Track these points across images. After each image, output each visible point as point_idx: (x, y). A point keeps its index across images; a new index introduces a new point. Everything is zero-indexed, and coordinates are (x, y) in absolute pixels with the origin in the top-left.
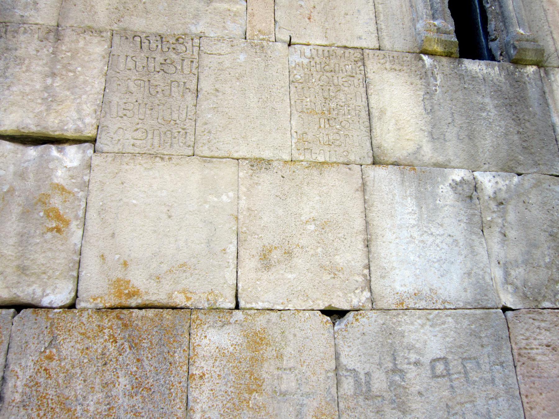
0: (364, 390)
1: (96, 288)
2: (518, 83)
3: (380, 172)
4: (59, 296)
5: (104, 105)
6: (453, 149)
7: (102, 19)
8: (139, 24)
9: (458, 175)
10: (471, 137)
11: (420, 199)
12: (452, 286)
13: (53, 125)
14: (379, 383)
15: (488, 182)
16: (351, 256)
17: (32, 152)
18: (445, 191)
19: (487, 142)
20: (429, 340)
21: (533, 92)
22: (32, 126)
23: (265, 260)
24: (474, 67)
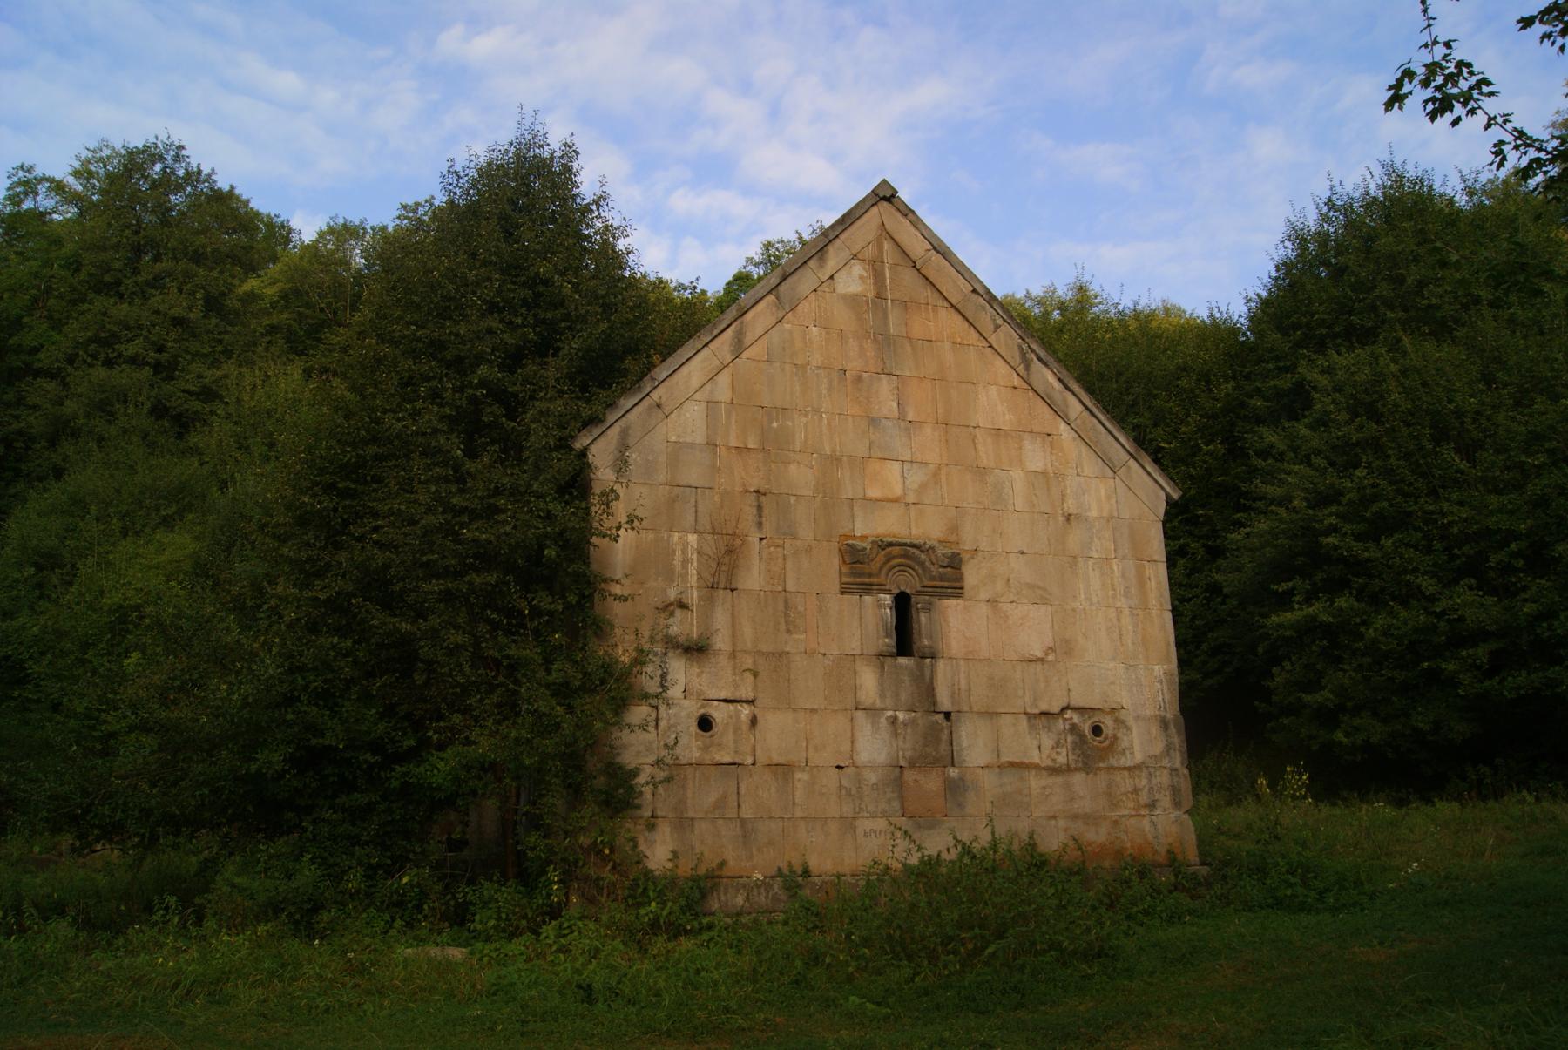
0: (849, 794)
1: (762, 758)
2: (921, 668)
3: (859, 713)
4: (749, 761)
5: (755, 688)
6: (889, 702)
7: (749, 645)
8: (764, 648)
9: (889, 713)
10: (897, 695)
11: (873, 724)
12: (882, 758)
13: (737, 696)
14: (854, 791)
15: (901, 716)
16: (846, 747)
17: (731, 707)
18: (883, 720)
19: (904, 697)
20: (872, 778)
21: (927, 673)
22: (730, 697)
23: (816, 749)
24: (902, 660)
